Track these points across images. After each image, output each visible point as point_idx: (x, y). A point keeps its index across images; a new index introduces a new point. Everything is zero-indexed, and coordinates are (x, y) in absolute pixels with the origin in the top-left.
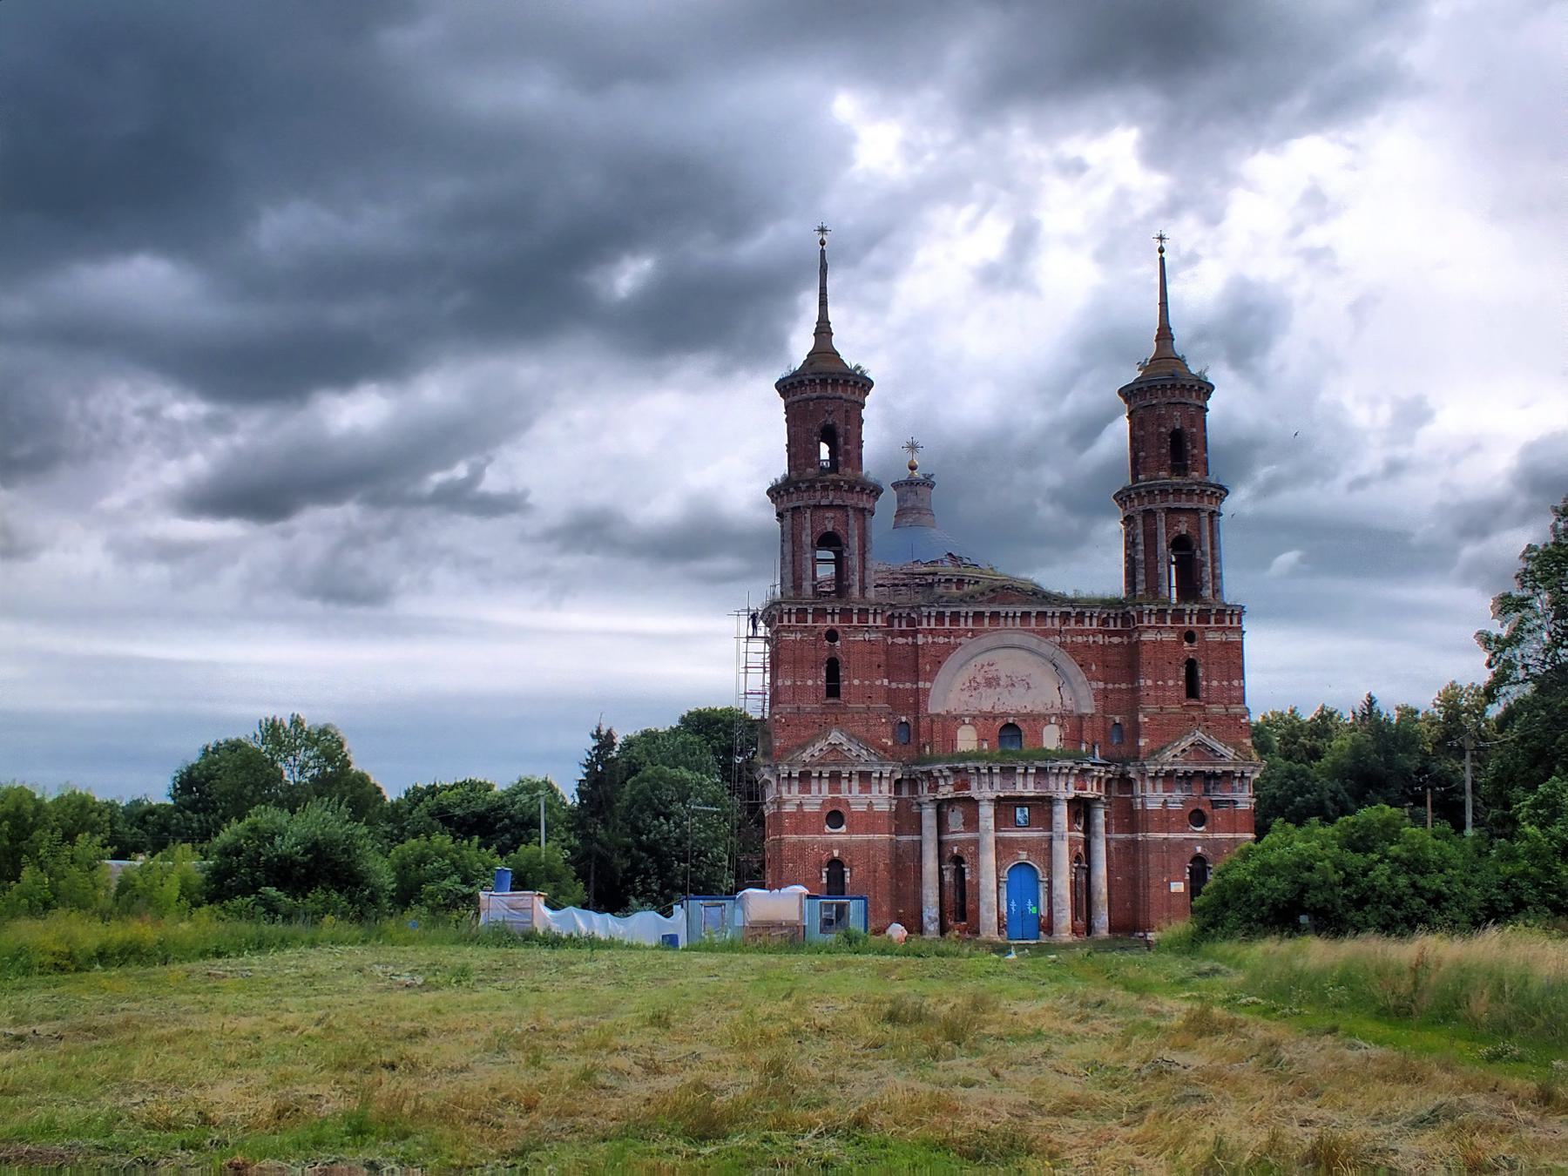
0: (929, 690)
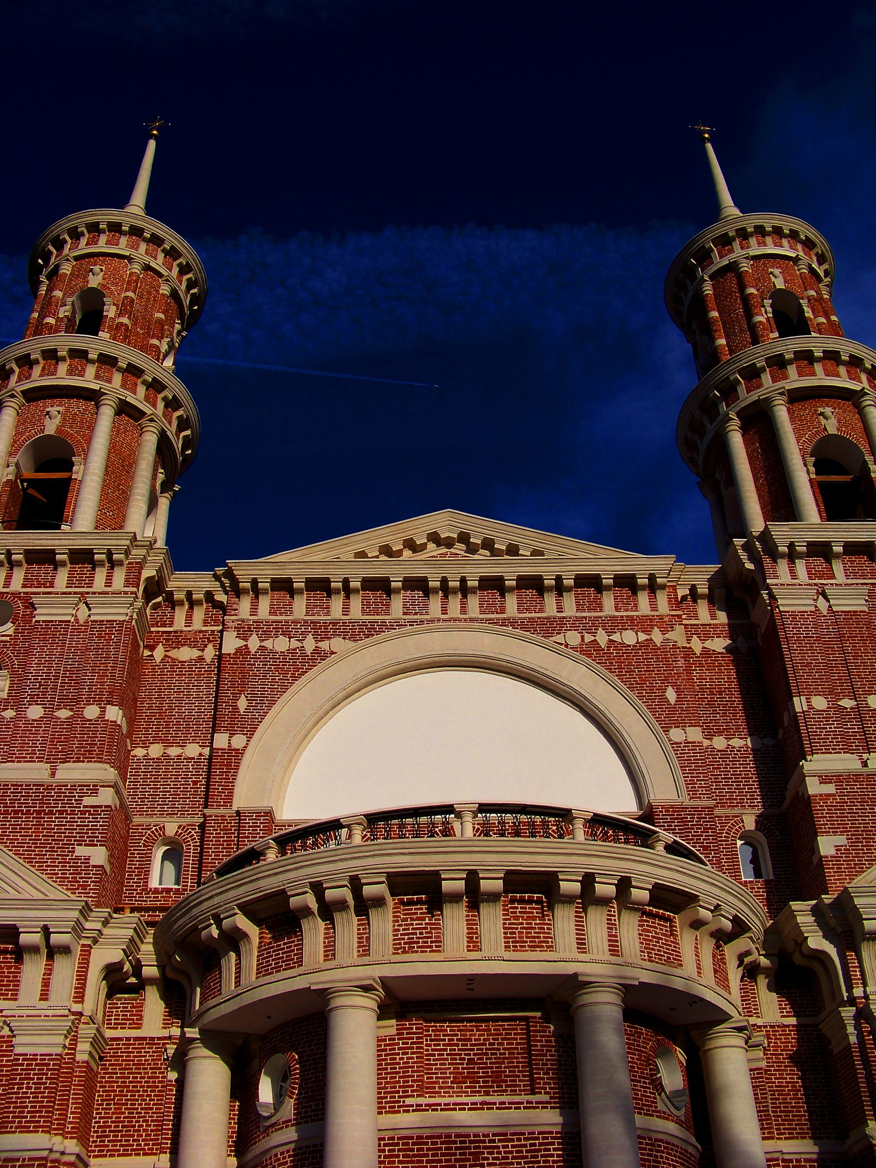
0: (239, 754)
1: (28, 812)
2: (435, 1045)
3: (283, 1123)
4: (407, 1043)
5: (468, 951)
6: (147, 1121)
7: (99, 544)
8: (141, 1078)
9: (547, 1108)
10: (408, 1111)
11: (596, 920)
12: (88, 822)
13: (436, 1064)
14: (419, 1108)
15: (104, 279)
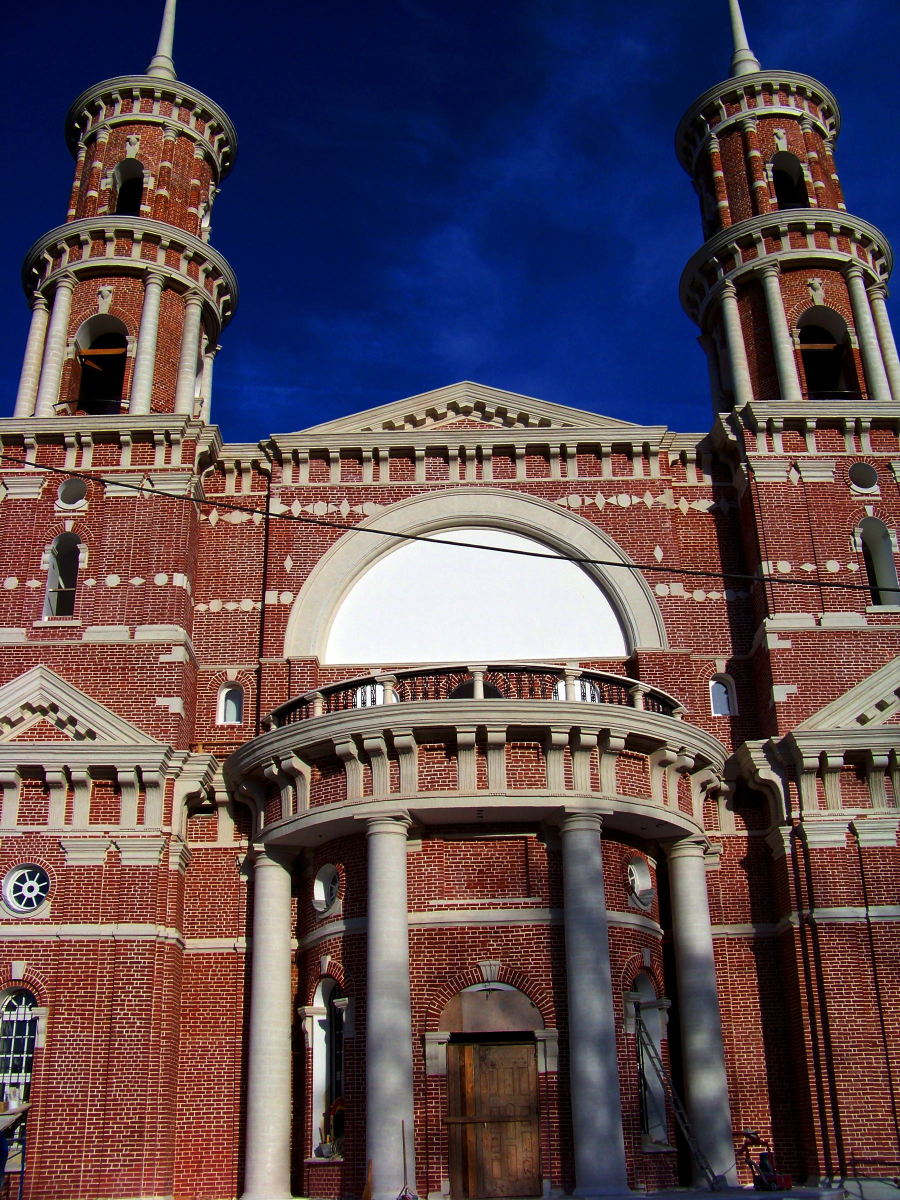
1: (114, 669)
2: (452, 859)
3: (335, 917)
4: (431, 858)
5: (478, 788)
6: (226, 912)
7: (158, 424)
8: (219, 880)
9: (540, 907)
10: (432, 910)
11: (581, 764)
12: (165, 676)
13: (454, 874)
14: (440, 908)
15: (141, 148)
